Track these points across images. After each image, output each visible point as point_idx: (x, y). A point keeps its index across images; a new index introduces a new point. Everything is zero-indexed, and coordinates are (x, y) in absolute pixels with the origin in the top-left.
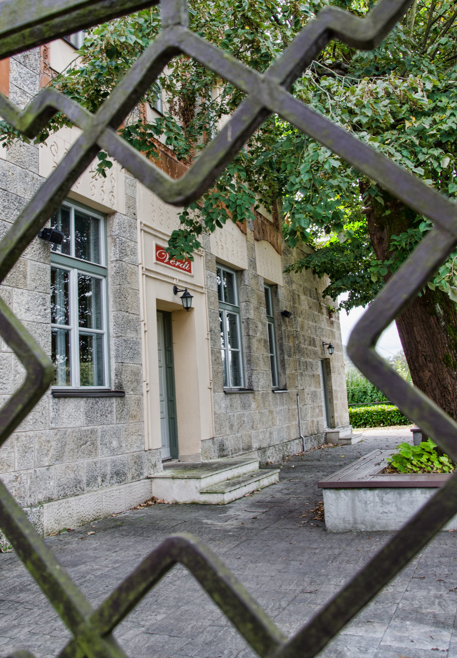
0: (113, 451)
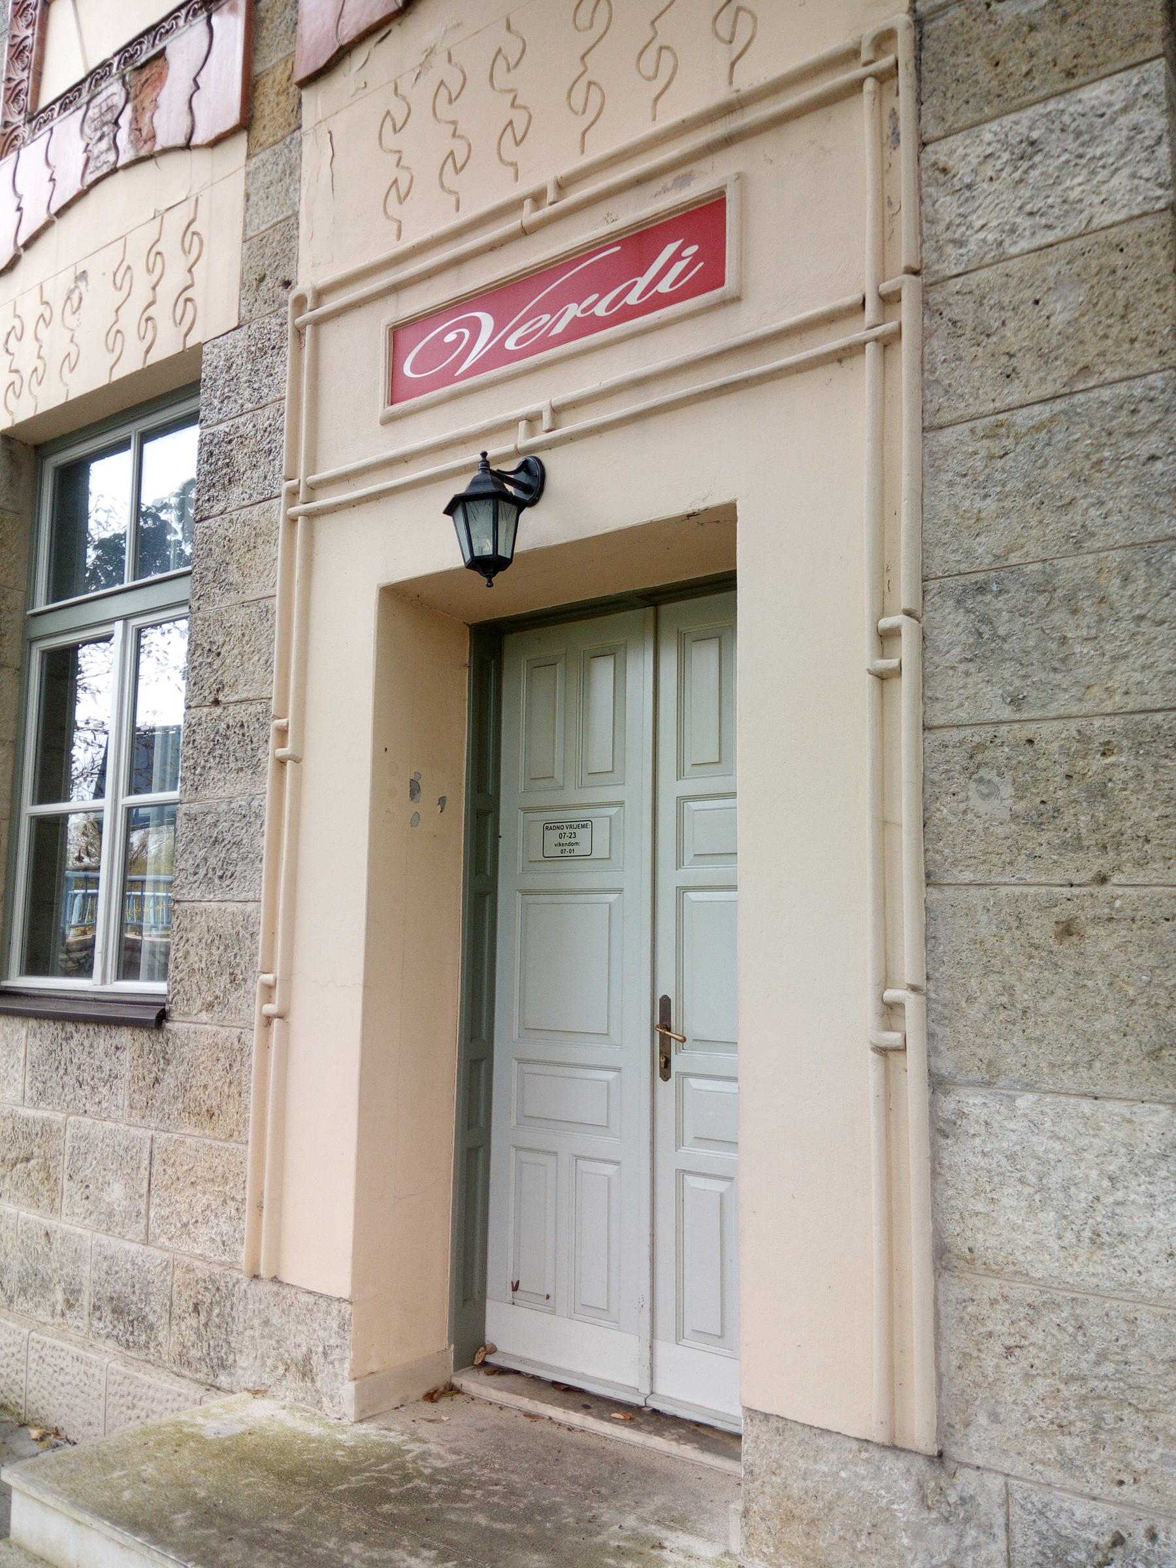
0: (109, 1220)
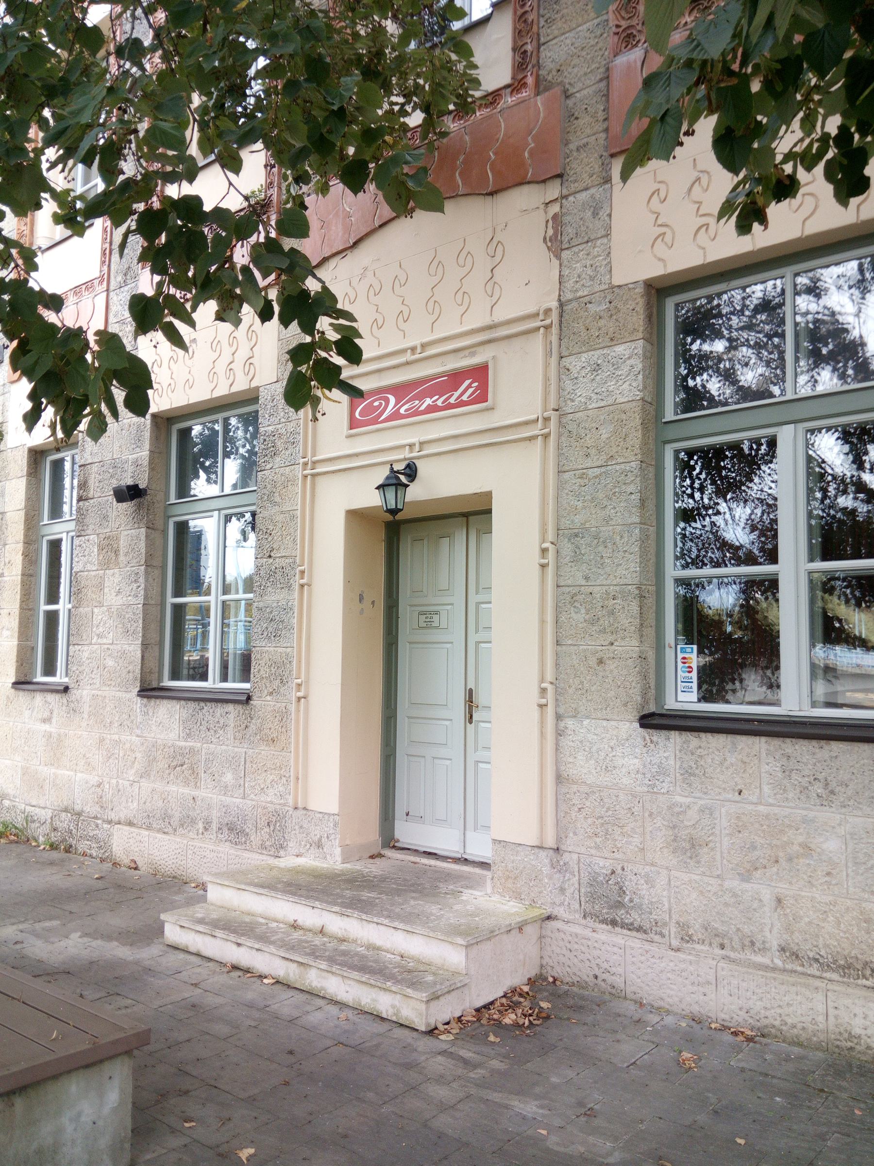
0: (226, 790)
